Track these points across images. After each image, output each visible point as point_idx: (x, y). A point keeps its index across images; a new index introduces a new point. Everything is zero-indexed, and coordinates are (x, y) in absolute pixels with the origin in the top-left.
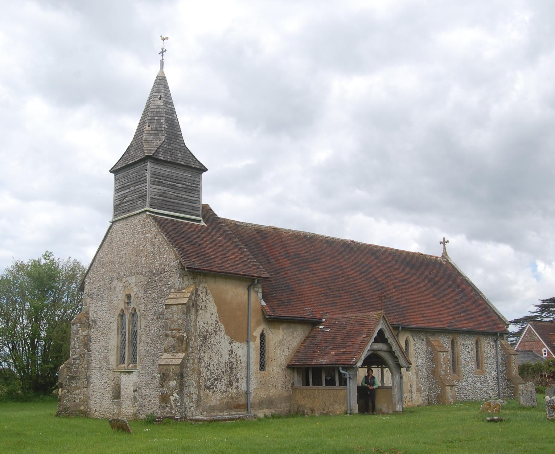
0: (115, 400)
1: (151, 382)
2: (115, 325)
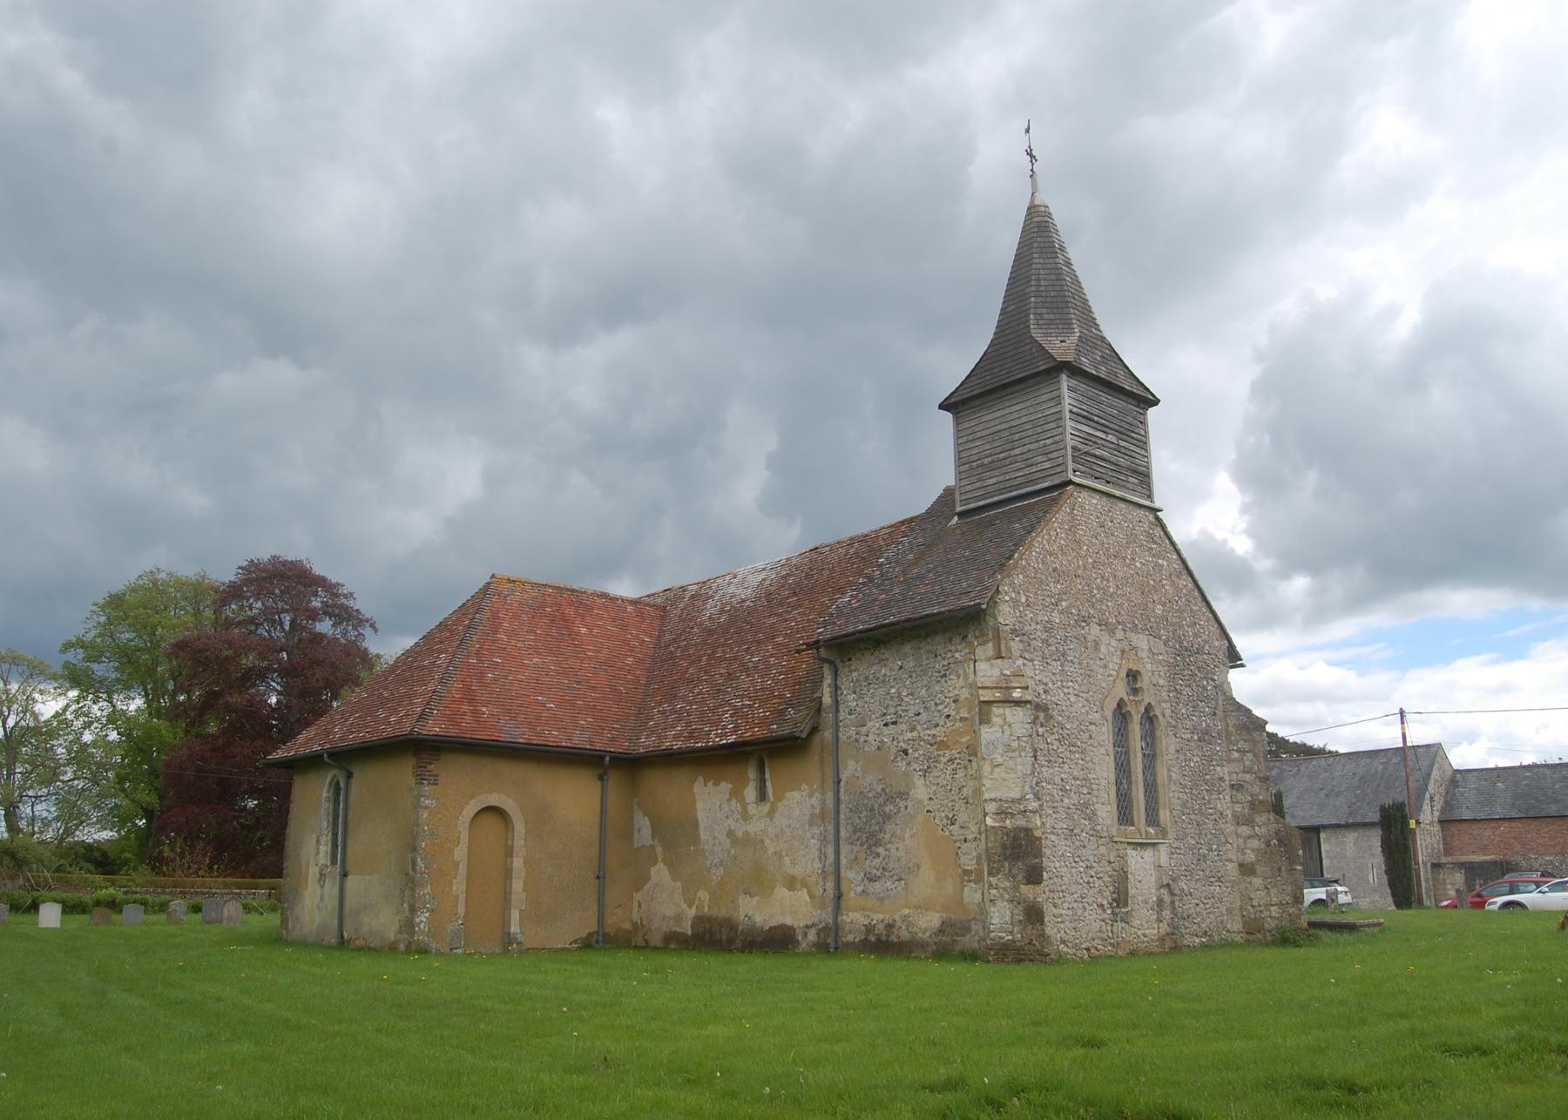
0: (1123, 910)
2: (1104, 729)
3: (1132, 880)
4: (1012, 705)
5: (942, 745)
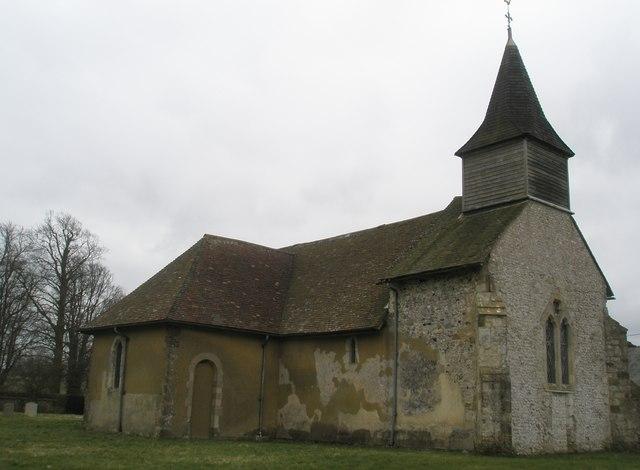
5: (456, 337)
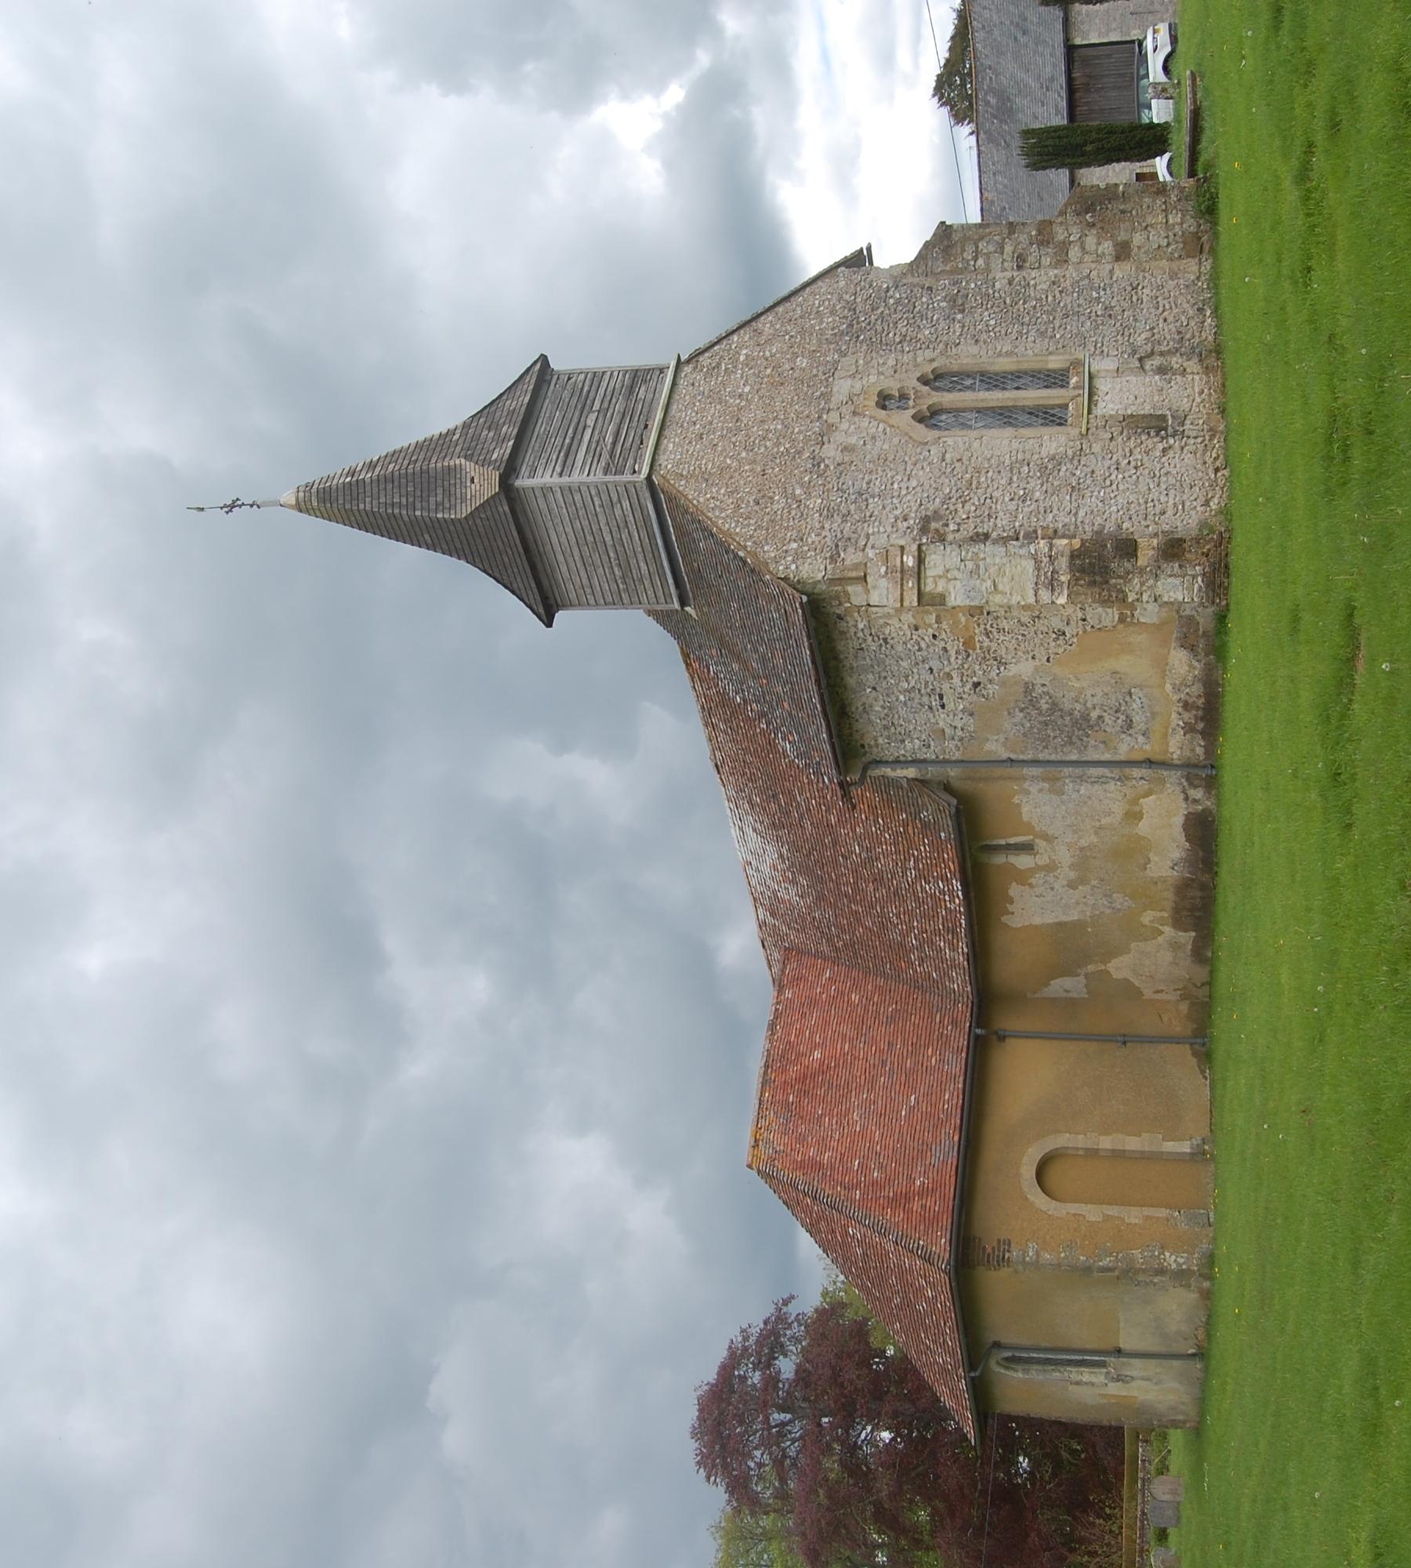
0: (1170, 422)
1: (1120, 317)
2: (950, 441)
3: (1133, 408)
4: (922, 568)
5: (969, 643)
